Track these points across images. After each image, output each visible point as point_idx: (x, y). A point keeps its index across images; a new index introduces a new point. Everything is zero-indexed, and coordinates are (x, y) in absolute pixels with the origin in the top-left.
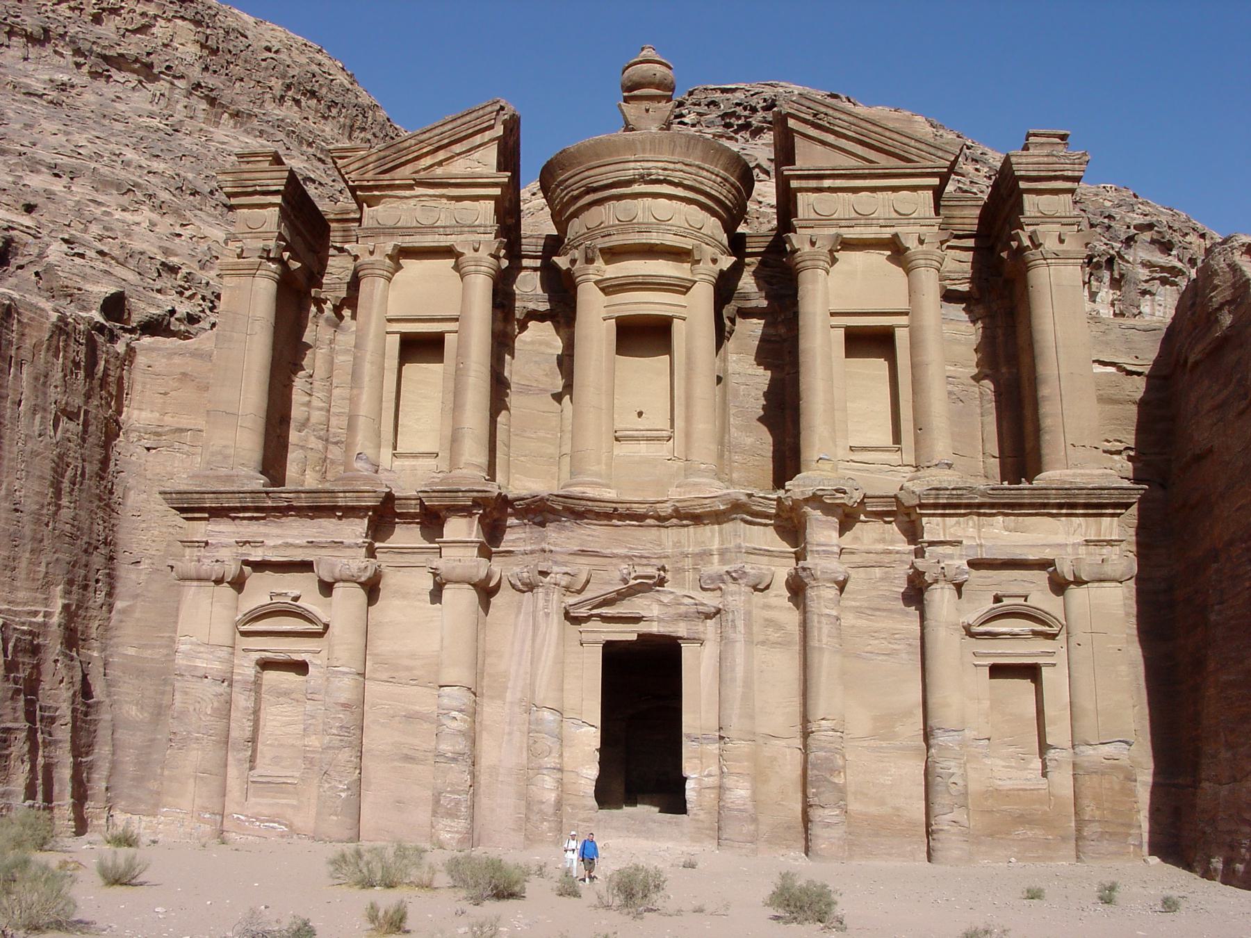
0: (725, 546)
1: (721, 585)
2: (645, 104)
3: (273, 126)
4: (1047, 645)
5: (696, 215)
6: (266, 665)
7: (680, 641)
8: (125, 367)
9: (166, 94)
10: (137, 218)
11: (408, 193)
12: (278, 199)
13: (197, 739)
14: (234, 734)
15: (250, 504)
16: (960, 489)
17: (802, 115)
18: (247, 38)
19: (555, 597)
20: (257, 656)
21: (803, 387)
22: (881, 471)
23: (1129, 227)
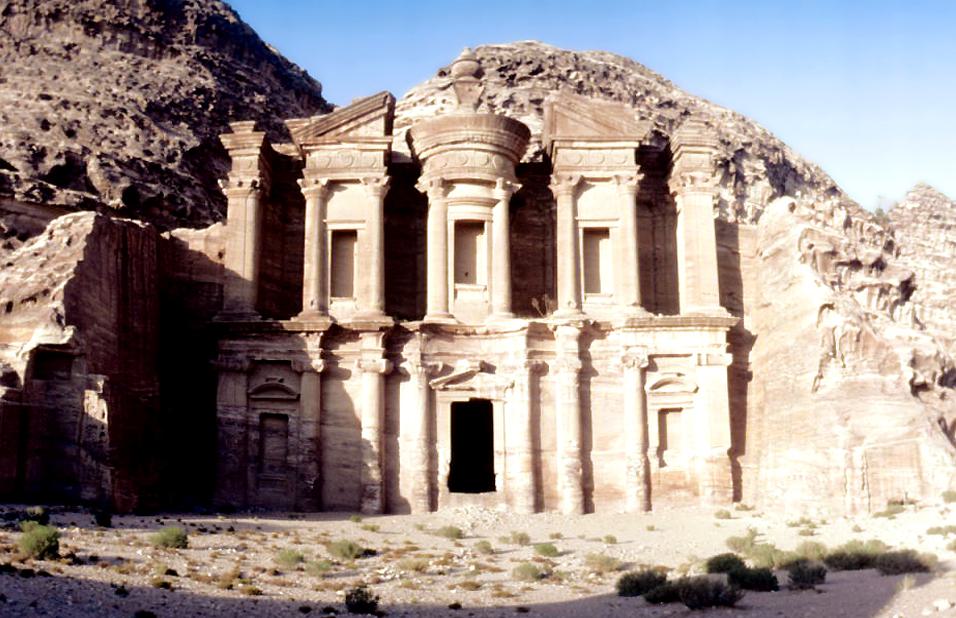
2: (467, 88)
4: (687, 398)
6: (263, 417)
19: (424, 379)
20: (259, 411)
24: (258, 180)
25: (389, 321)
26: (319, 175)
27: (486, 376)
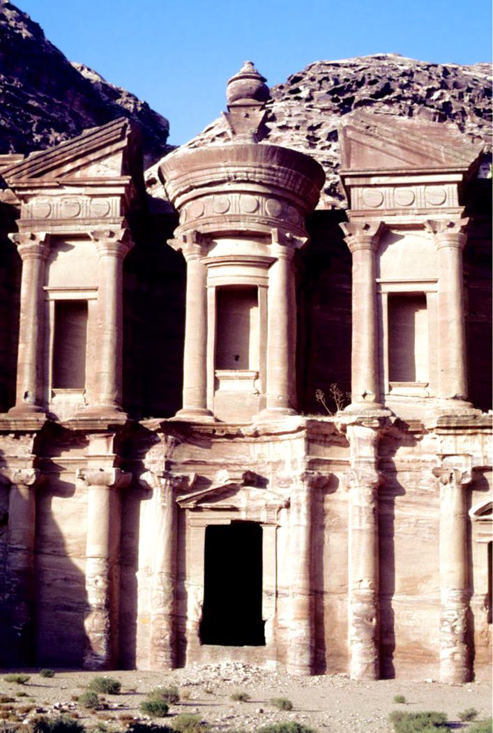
7: (261, 525)
25: (122, 418)
27: (254, 491)
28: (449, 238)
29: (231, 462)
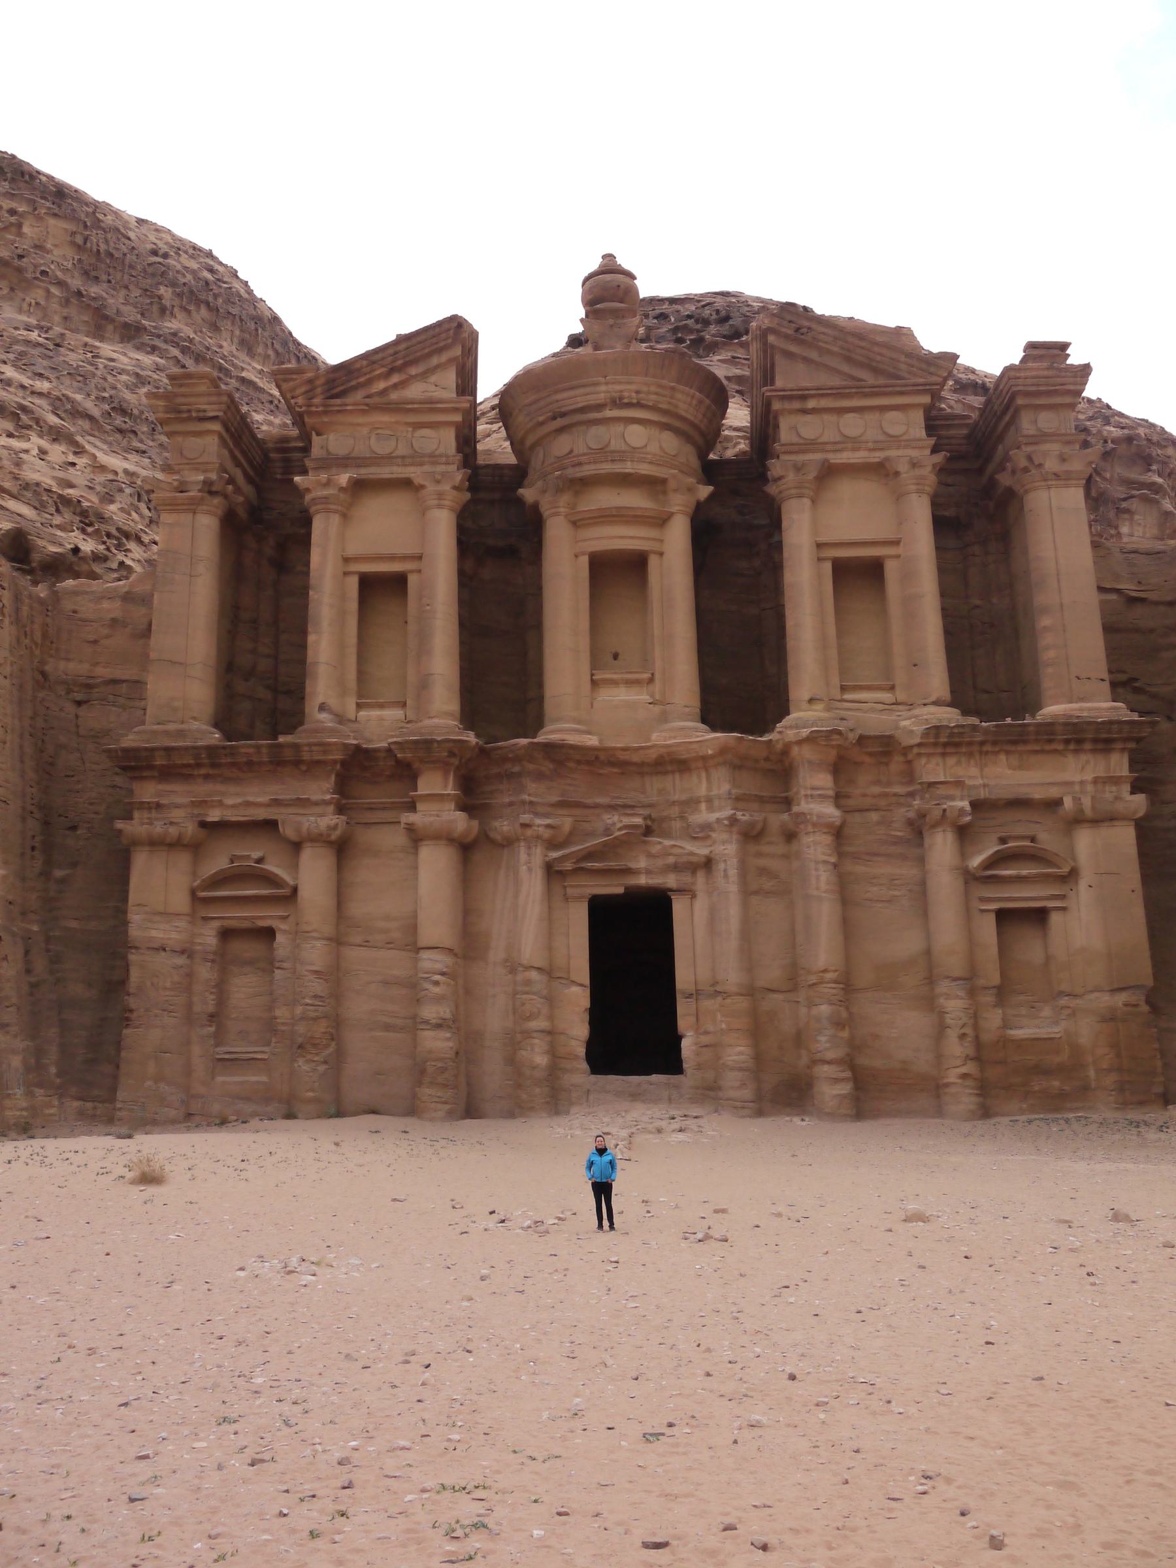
0: (715, 792)
1: (710, 833)
3: (166, 341)
5: (669, 442)
7: (669, 893)
8: (49, 613)
9: (42, 303)
10: (24, 445)
11: (360, 419)
12: (216, 427)
13: (156, 1016)
14: (197, 1008)
15: (206, 761)
16: (963, 726)
17: (783, 330)
18: (129, 239)
20: (216, 924)
21: (790, 623)
22: (873, 710)
23: (1106, 442)
24: (213, 476)
25: (471, 737)
26: (334, 470)
27: (658, 844)
28: (914, 481)
29: (619, 802)
